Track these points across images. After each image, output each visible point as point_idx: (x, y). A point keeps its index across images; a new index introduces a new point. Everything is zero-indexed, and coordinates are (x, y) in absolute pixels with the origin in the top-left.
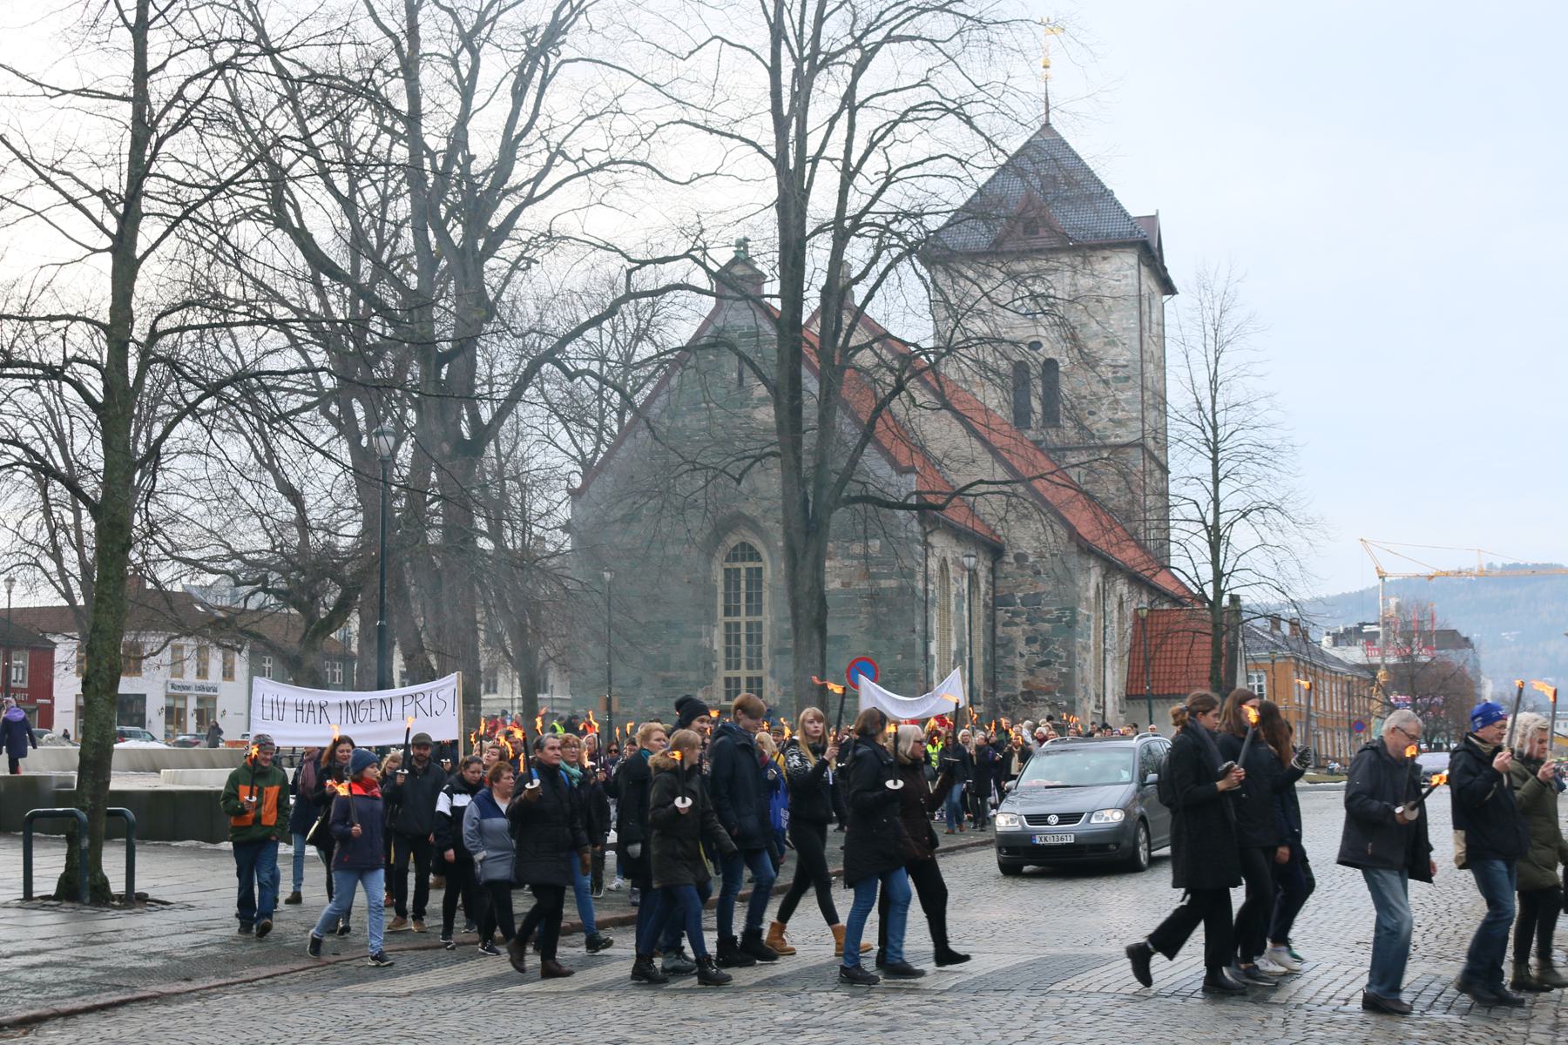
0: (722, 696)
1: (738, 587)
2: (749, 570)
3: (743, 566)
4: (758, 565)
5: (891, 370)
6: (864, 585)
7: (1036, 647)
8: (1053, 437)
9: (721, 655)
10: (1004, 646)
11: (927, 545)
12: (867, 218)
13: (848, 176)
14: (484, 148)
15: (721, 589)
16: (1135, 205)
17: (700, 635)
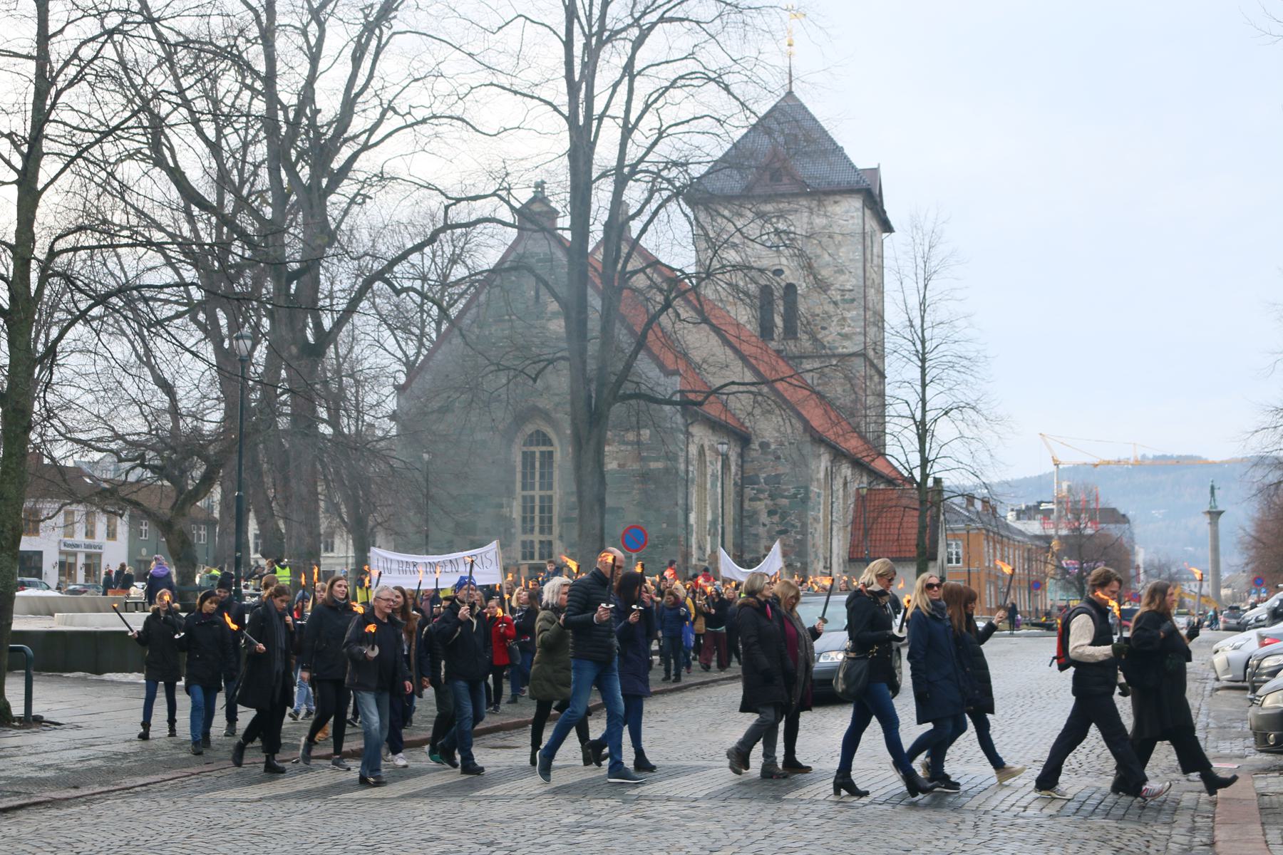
0: (519, 556)
2: (542, 453)
3: (537, 450)
4: (550, 449)
5: (661, 290)
6: (636, 466)
7: (776, 519)
8: (792, 347)
9: (518, 523)
10: (749, 517)
11: (688, 435)
12: (642, 166)
13: (627, 131)
14: (328, 104)
15: (519, 468)
16: (861, 159)
17: (501, 506)
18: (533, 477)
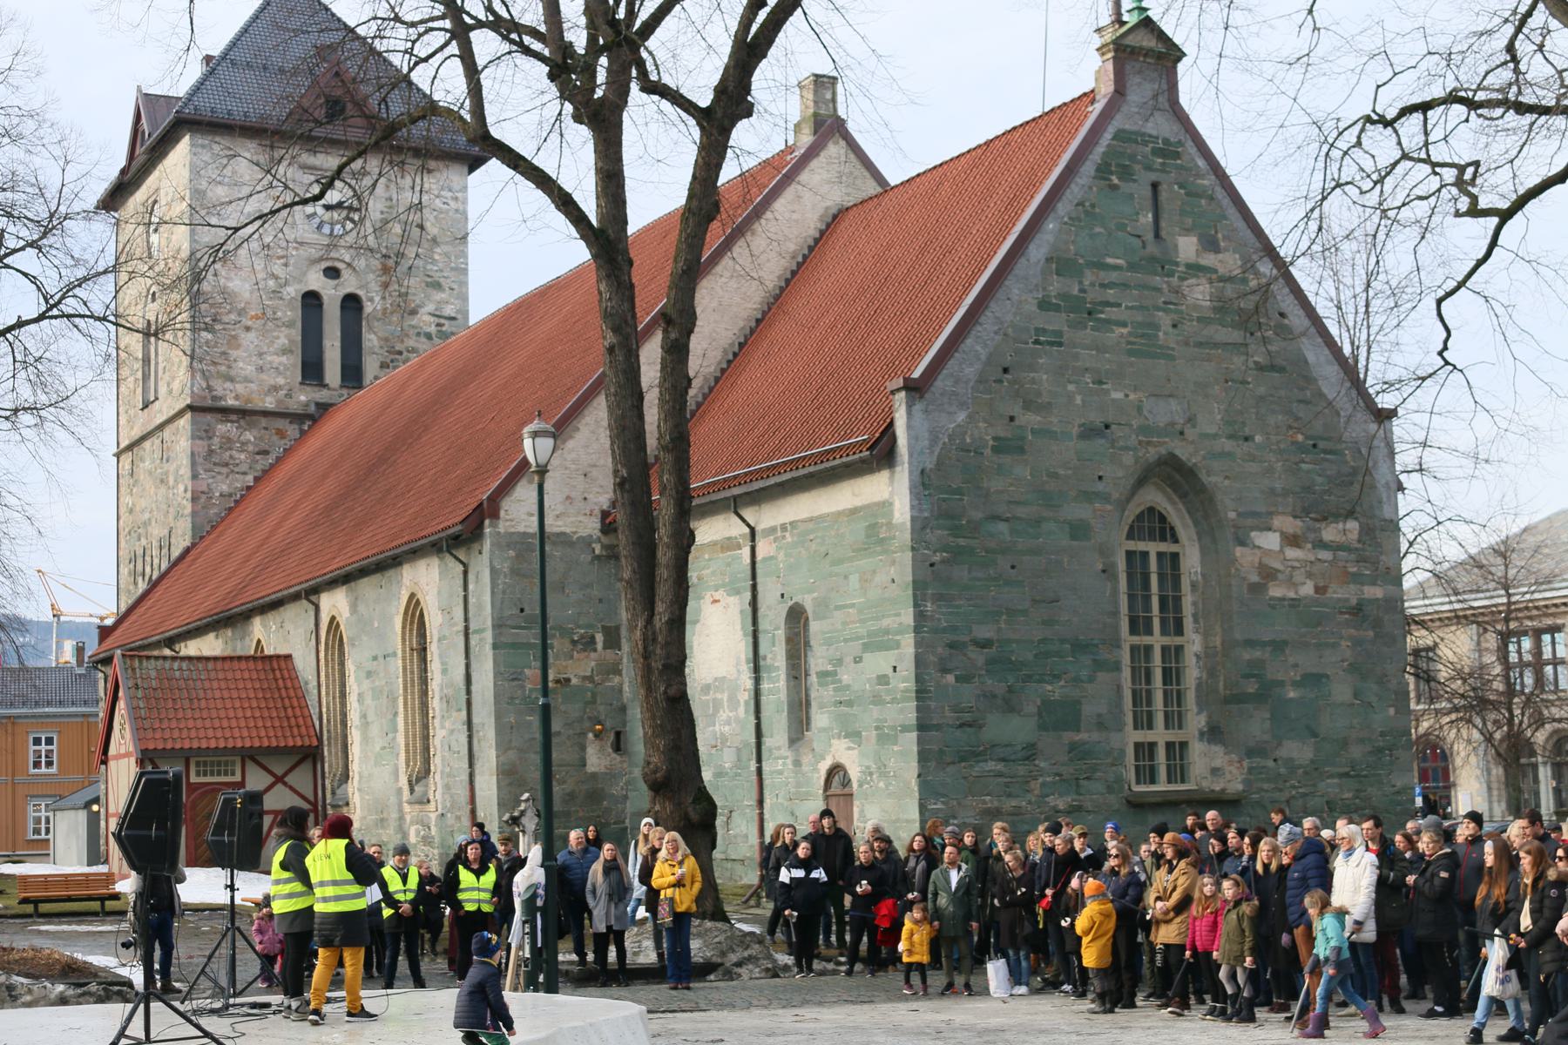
0: (1131, 775)
1: (1146, 585)
2: (1160, 555)
3: (1153, 548)
4: (1173, 548)
18: (1148, 608)
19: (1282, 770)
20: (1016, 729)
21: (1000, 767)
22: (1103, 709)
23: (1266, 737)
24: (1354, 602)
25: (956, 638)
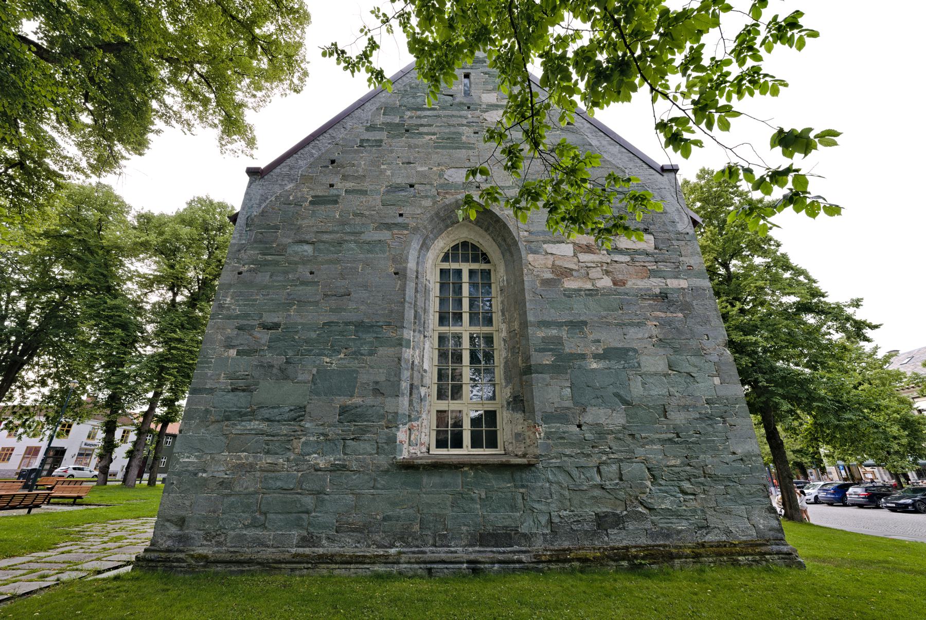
9: (432, 377)
15: (435, 290)
19: (588, 436)
20: (288, 394)
21: (263, 426)
22: (382, 378)
23: (568, 404)
24: (658, 291)
25: (245, 322)
